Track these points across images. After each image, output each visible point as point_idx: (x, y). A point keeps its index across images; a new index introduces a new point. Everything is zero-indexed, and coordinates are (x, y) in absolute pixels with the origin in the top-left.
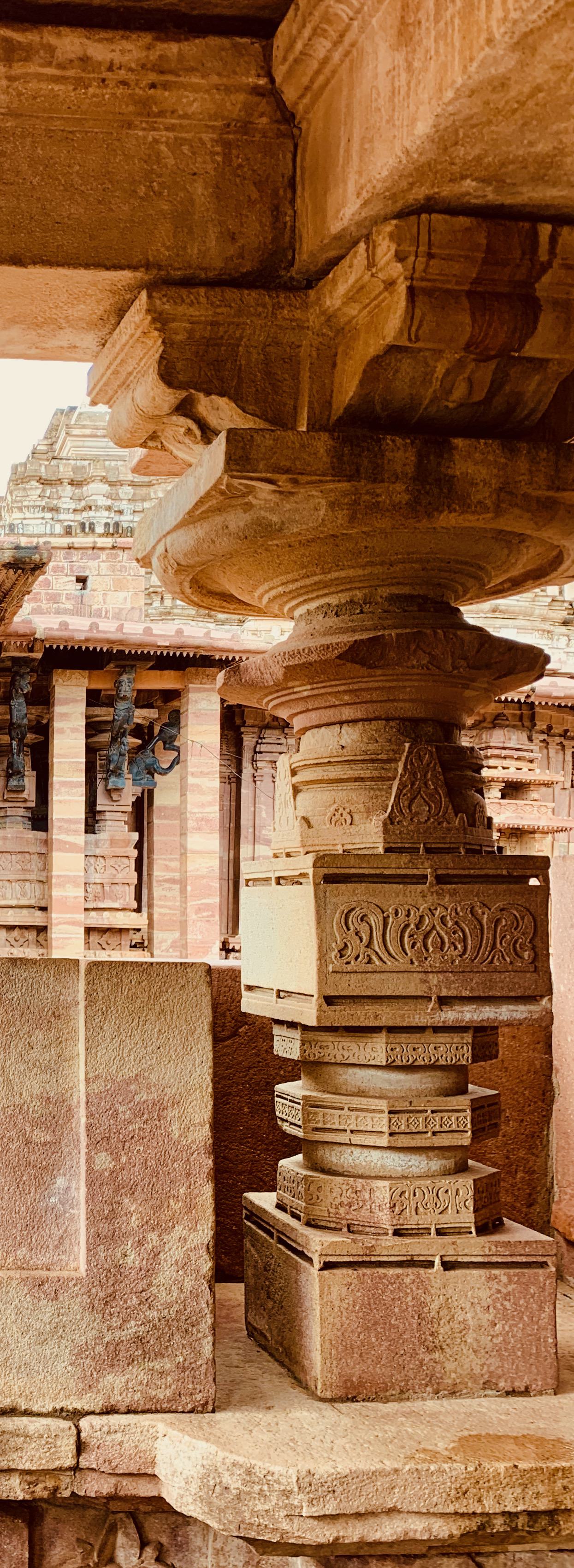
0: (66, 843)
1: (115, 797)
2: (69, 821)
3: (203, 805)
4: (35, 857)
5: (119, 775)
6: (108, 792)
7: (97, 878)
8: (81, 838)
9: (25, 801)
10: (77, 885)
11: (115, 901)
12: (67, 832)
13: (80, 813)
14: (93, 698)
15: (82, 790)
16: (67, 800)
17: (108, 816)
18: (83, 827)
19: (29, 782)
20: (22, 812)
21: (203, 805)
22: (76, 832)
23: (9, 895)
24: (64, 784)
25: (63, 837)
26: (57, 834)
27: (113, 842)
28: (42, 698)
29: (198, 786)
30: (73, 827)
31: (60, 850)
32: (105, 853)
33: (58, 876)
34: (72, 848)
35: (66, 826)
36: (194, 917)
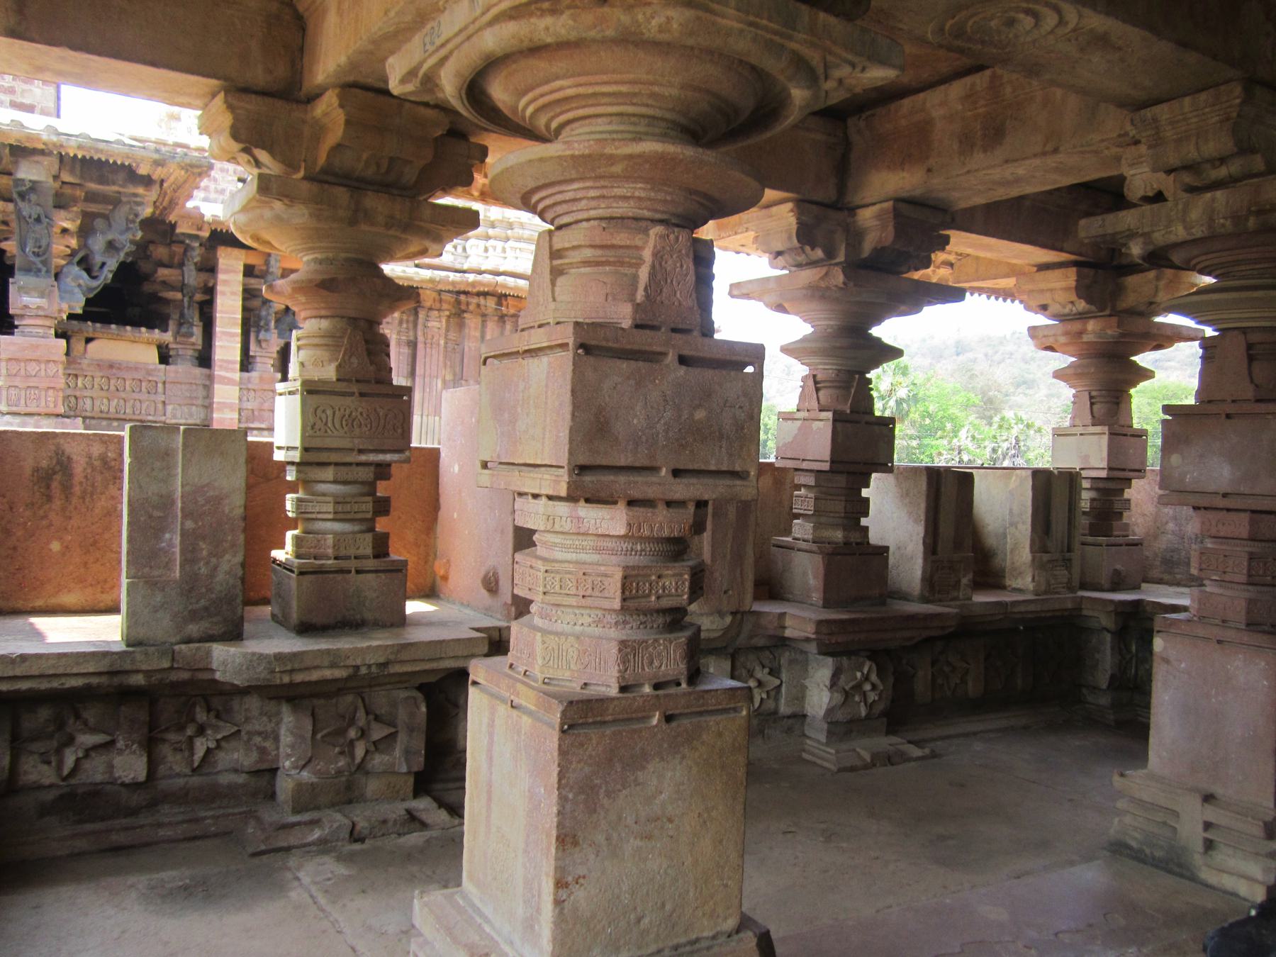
1: (264, 345)
4: (201, 388)
5: (267, 330)
6: (259, 342)
7: (249, 405)
8: (237, 375)
9: (193, 344)
10: (232, 410)
11: (262, 422)
12: (227, 370)
13: (237, 356)
14: (249, 271)
15: (239, 339)
16: (227, 346)
17: (258, 359)
18: (238, 366)
19: (197, 331)
20: (190, 352)
22: (233, 370)
24: (224, 333)
25: (223, 373)
26: (218, 372)
27: (261, 378)
28: (209, 268)
30: (231, 366)
34: (230, 382)
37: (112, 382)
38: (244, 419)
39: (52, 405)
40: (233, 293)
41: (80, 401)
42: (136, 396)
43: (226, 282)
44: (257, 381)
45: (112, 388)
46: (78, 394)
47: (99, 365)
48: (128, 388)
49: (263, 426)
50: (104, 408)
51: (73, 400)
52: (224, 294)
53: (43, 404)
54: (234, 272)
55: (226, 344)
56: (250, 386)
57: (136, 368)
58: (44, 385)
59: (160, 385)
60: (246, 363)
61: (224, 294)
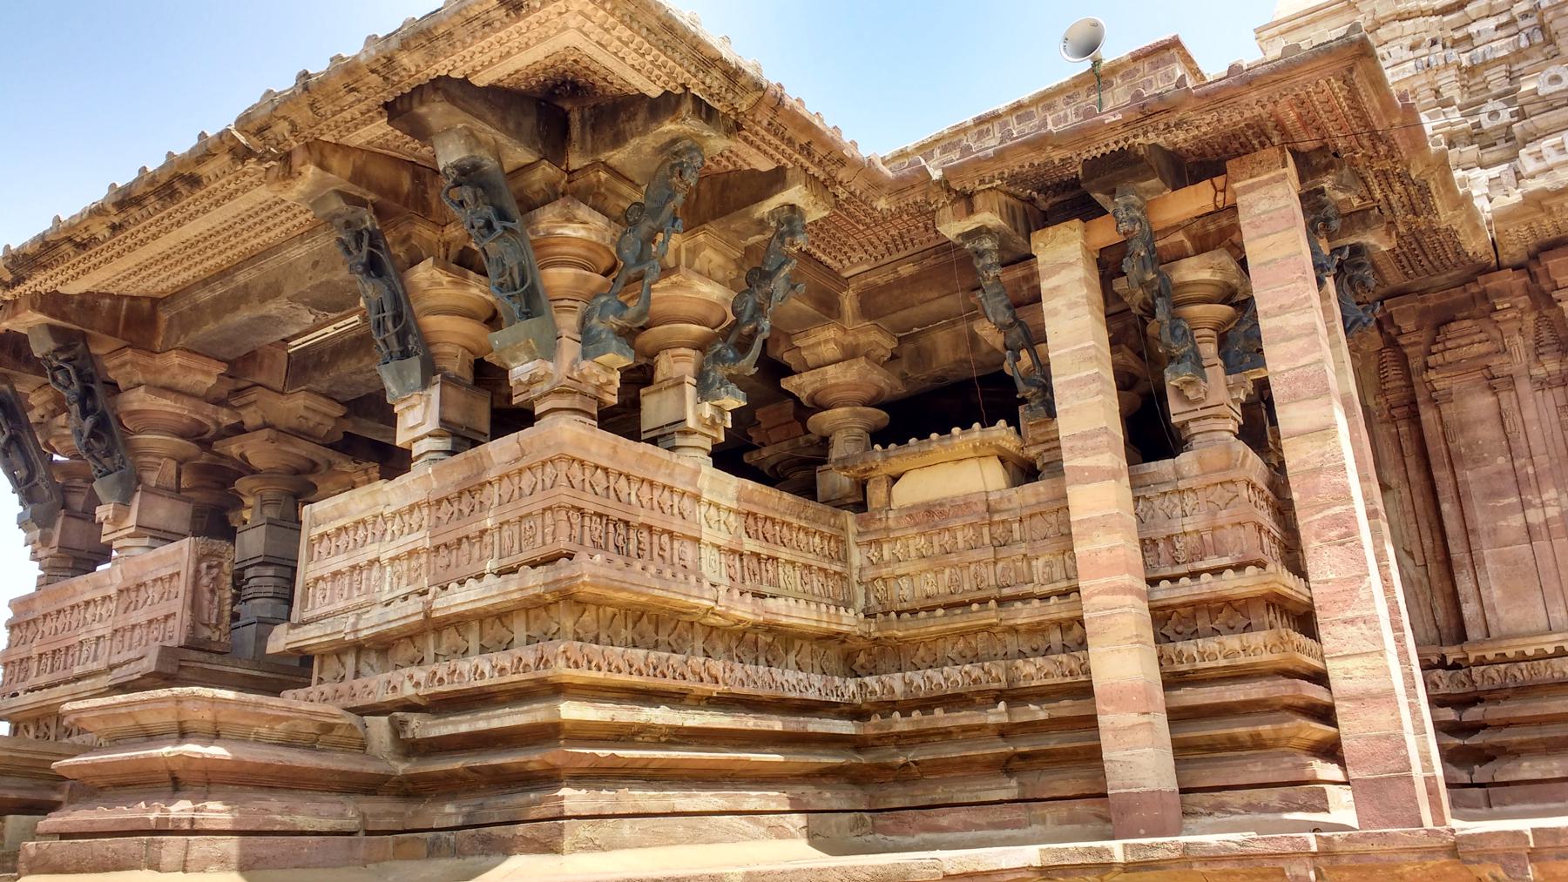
0: (1083, 469)
2: (1084, 436)
3: (1294, 357)
12: (1084, 452)
17: (1193, 428)
21: (1294, 357)
23: (1057, 576)
24: (1069, 384)
25: (1078, 462)
29: (1279, 329)
31: (1077, 482)
32: (1194, 483)
33: (1080, 522)
34: (1096, 475)
35: (1079, 444)
36: (1316, 543)
37: (935, 539)
38: (1183, 556)
39: (549, 539)
40: (1072, 305)
41: (892, 583)
42: (975, 555)
43: (1055, 289)
44: (1196, 470)
45: (937, 549)
46: (884, 572)
47: (910, 512)
48: (961, 545)
49: (1226, 561)
50: (930, 590)
51: (879, 584)
52: (1055, 313)
53: (539, 540)
54: (1067, 265)
55: (1076, 403)
56: (1181, 485)
57: (962, 505)
58: (537, 508)
59: (1016, 526)
60: (1150, 434)
61: (1055, 313)
